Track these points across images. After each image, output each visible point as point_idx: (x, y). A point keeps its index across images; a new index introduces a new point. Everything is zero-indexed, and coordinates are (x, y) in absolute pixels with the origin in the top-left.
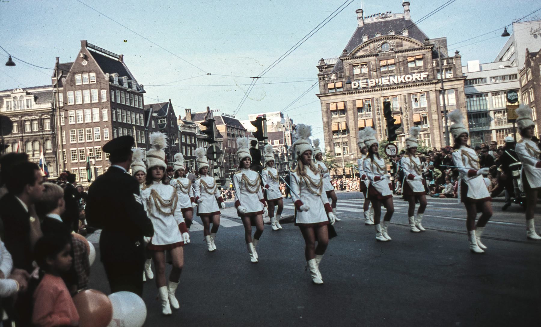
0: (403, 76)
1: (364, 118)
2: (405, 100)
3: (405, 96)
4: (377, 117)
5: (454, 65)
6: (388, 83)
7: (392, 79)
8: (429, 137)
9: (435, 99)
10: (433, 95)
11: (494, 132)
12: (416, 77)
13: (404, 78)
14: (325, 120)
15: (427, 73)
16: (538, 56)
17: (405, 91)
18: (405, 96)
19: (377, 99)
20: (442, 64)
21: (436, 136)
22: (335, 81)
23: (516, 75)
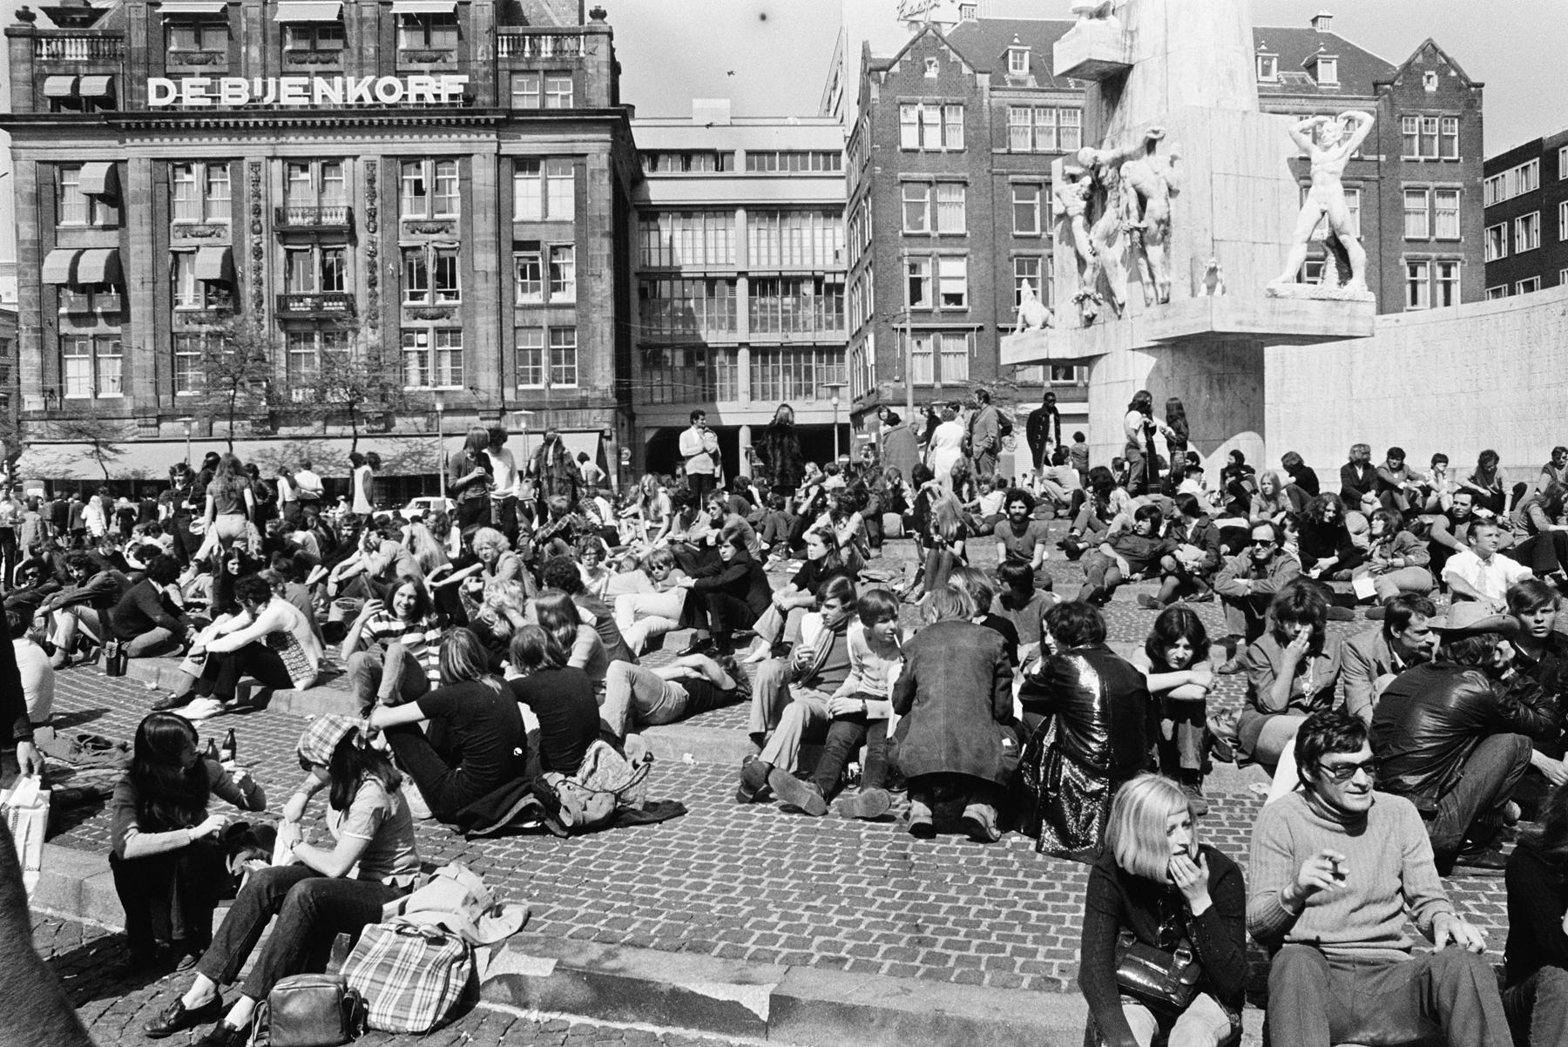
0: (369, 79)
1: (197, 241)
2: (372, 181)
3: (371, 165)
4: (249, 241)
5: (580, 60)
6: (306, 101)
7: (319, 83)
8: (455, 342)
9: (492, 190)
10: (483, 174)
11: (744, 354)
12: (420, 90)
13: (372, 88)
14: (28, 232)
15: (465, 79)
16: (896, 69)
17: (373, 147)
18: (371, 165)
19: (255, 166)
21: (482, 341)
22: (82, 70)
23: (838, 154)
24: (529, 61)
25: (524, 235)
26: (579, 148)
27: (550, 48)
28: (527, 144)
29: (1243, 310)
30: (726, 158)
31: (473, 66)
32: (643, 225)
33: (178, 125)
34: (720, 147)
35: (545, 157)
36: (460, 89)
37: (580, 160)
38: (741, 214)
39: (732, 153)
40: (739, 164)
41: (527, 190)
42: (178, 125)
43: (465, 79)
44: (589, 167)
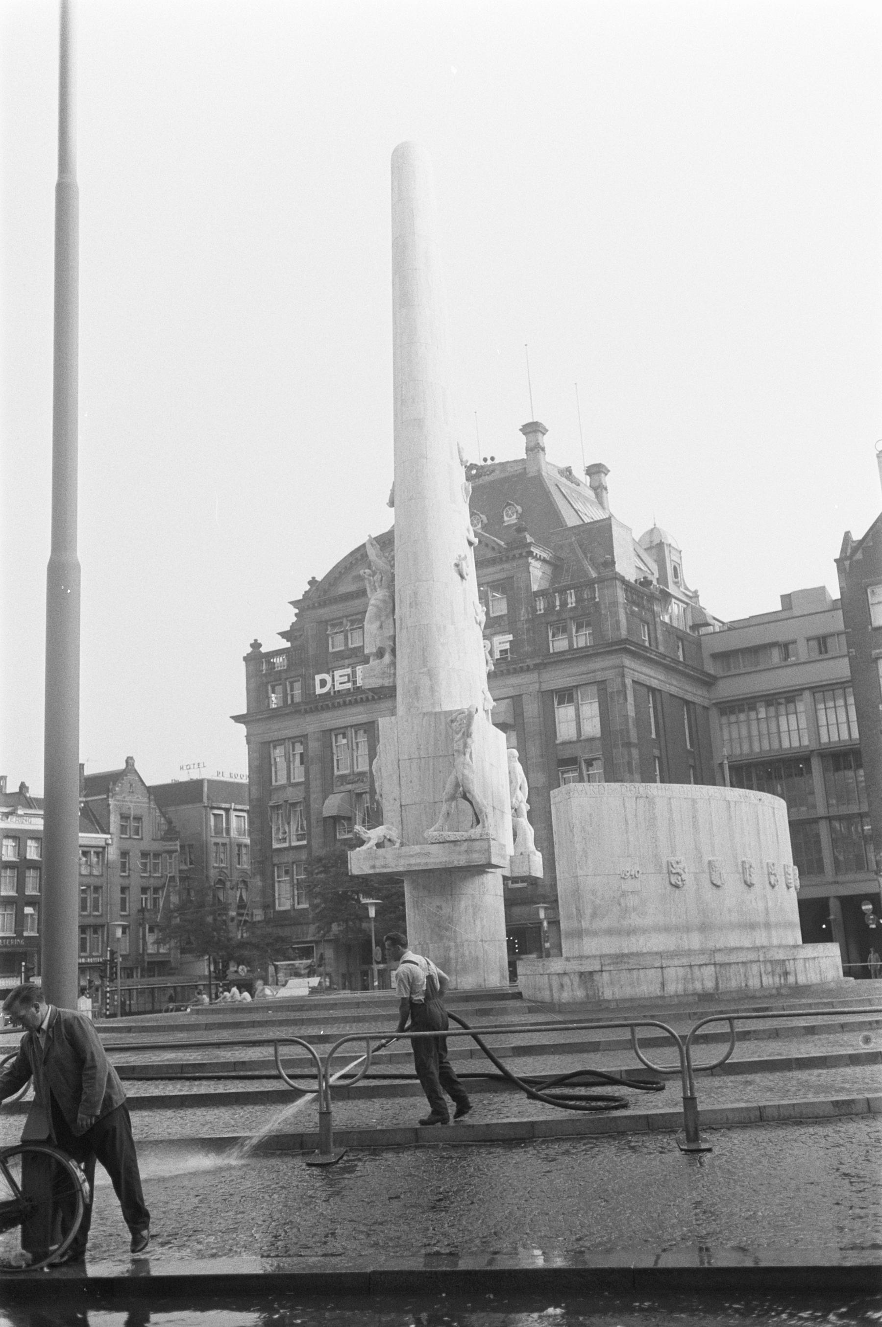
20: (564, 604)
24: (559, 612)
25: (567, 754)
26: (599, 676)
27: (574, 599)
28: (558, 679)
29: (376, 858)
30: (791, 647)
31: (519, 625)
32: (724, 720)
33: (333, 705)
34: (781, 639)
35: (577, 687)
36: (507, 646)
37: (602, 686)
38: (807, 695)
39: (794, 642)
40: (802, 651)
41: (565, 714)
42: (333, 705)
43: (510, 637)
44: (609, 690)
